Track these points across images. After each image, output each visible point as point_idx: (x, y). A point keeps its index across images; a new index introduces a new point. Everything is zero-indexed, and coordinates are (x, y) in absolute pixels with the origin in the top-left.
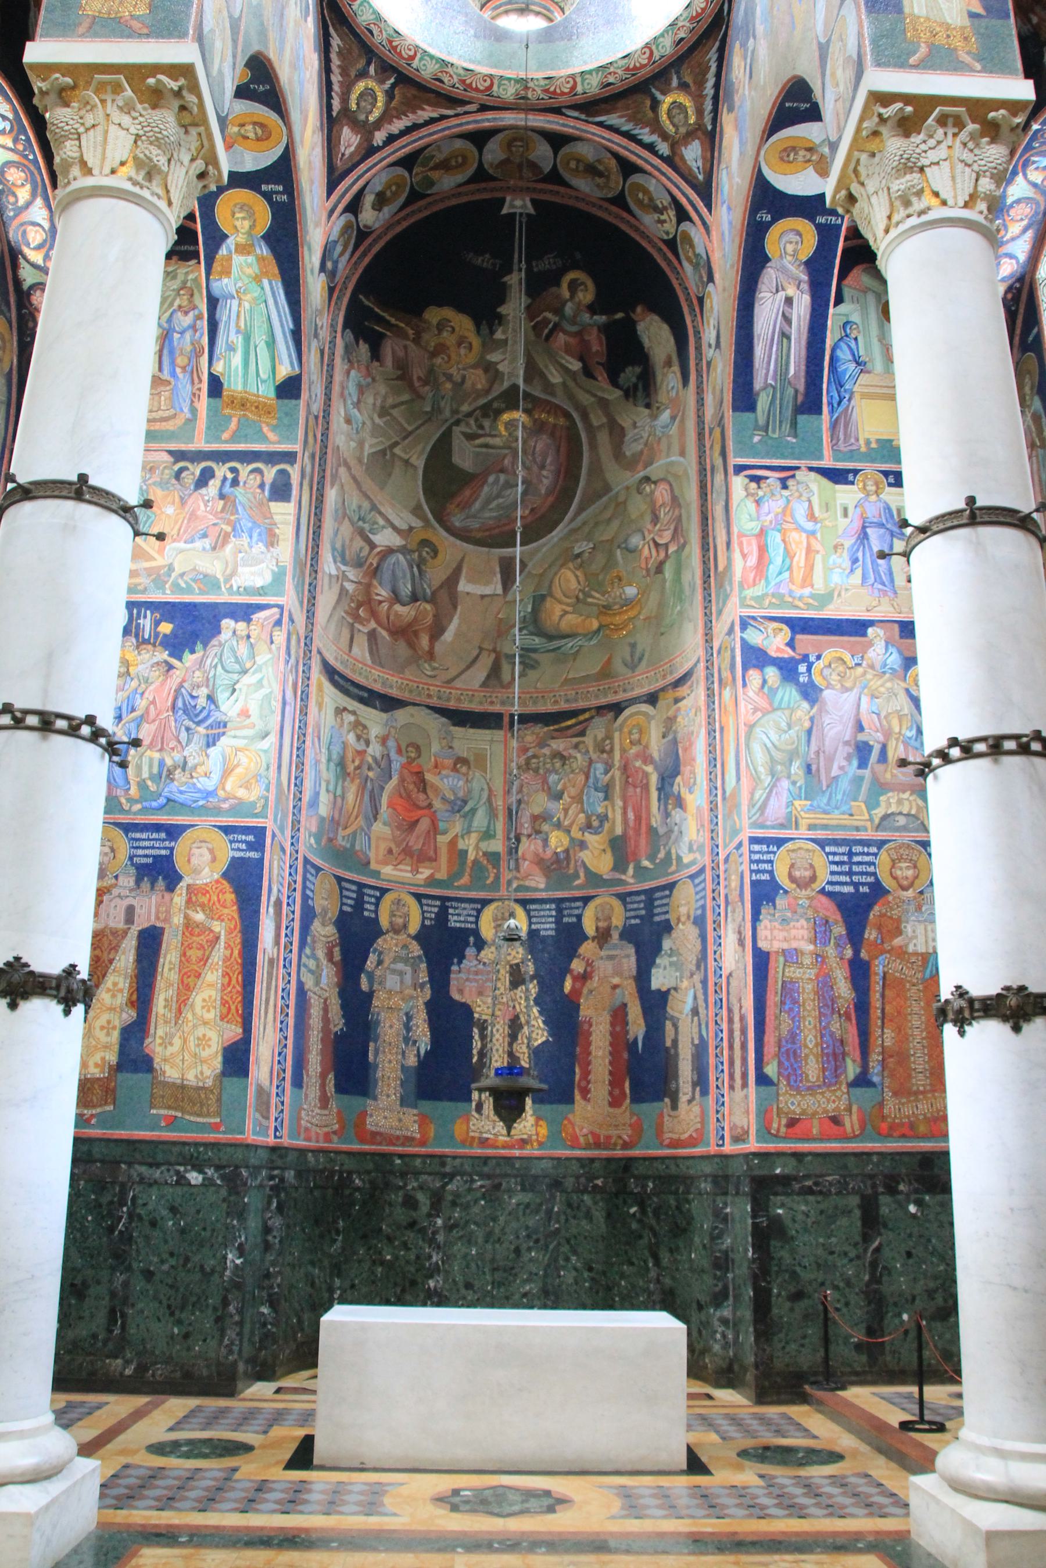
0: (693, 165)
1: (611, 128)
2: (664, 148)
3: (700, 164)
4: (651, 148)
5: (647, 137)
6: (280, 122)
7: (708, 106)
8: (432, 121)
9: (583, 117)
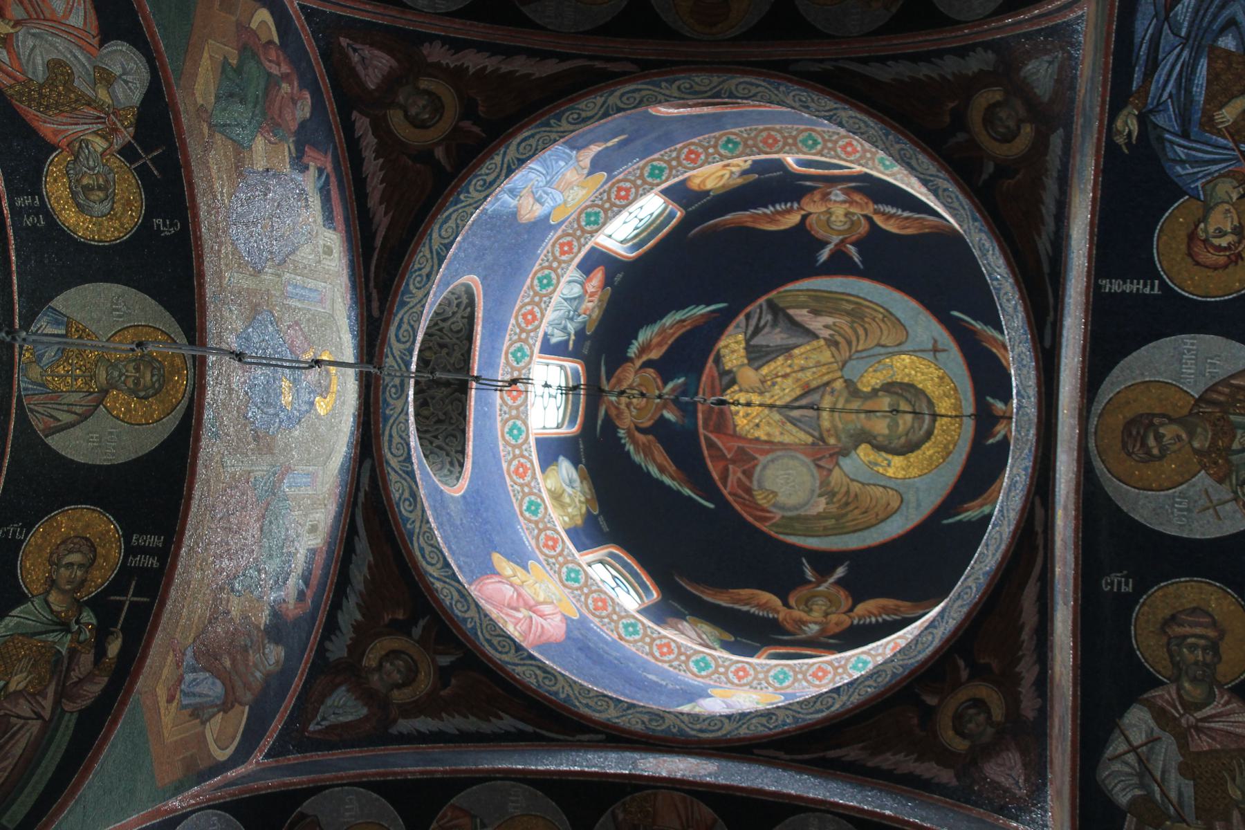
0: (367, 52)
1: (544, 55)
2: (436, 54)
3: (356, 58)
4: (457, 45)
5: (473, 61)
6: (1098, 464)
7: (369, 143)
8: (882, 60)
9: (598, 64)
